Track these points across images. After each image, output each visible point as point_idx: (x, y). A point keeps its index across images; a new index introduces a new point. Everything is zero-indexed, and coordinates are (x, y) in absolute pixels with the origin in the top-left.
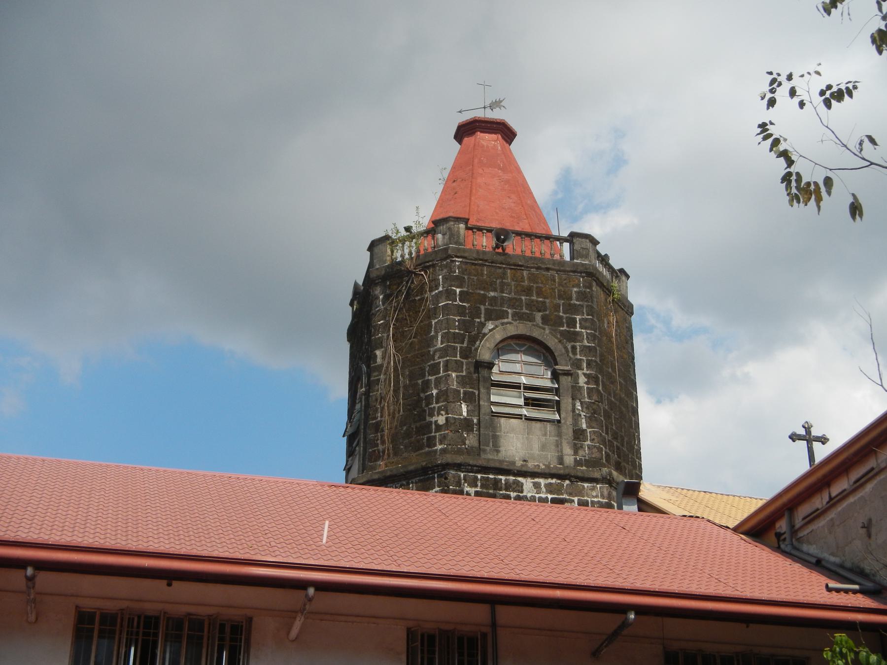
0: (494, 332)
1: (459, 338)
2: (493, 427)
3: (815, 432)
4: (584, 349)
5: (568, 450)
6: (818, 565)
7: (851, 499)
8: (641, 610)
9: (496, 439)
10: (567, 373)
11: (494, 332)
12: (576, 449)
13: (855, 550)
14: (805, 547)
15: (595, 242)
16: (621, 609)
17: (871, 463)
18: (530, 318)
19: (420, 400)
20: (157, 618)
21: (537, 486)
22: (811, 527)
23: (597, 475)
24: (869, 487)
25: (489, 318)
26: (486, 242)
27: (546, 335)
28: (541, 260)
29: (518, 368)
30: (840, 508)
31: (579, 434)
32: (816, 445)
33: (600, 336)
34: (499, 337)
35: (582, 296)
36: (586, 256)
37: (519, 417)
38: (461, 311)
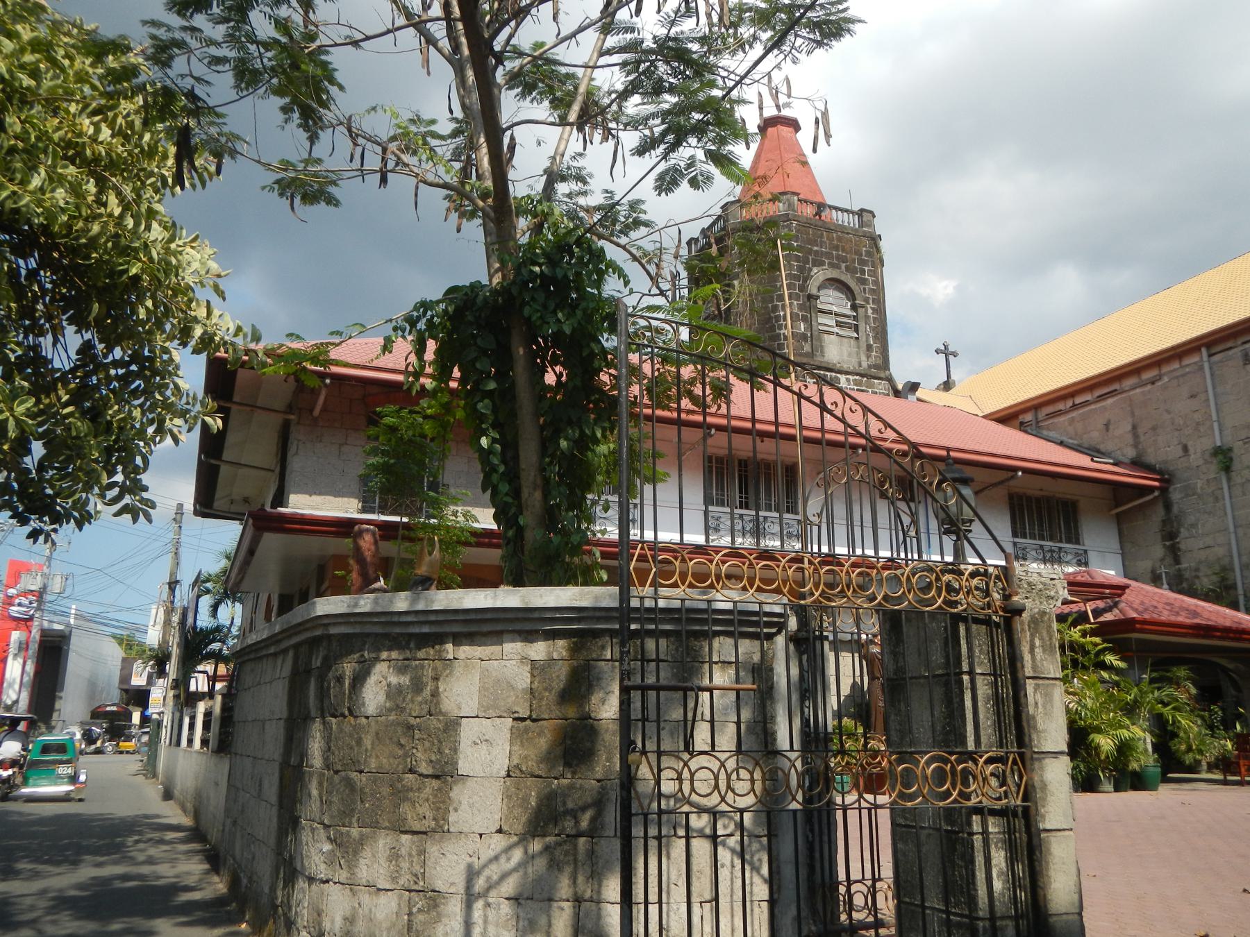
0: (819, 274)
1: (797, 278)
2: (820, 340)
3: (951, 349)
4: (871, 290)
5: (864, 358)
6: (1061, 443)
7: (1093, 407)
8: (1025, 470)
9: (822, 347)
10: (862, 307)
11: (819, 274)
12: (868, 357)
13: (1094, 437)
14: (1045, 433)
15: (874, 216)
16: (1014, 469)
17: (1116, 386)
18: (839, 267)
19: (770, 318)
20: (746, 461)
21: (848, 380)
22: (1051, 421)
23: (882, 375)
24: (1110, 401)
25: (814, 265)
26: (809, 211)
27: (847, 278)
28: (843, 226)
29: (831, 300)
30: (1081, 411)
31: (869, 348)
32: (951, 357)
33: (876, 283)
34: (821, 279)
35: (869, 254)
36: (870, 226)
37: (832, 333)
38: (797, 259)
